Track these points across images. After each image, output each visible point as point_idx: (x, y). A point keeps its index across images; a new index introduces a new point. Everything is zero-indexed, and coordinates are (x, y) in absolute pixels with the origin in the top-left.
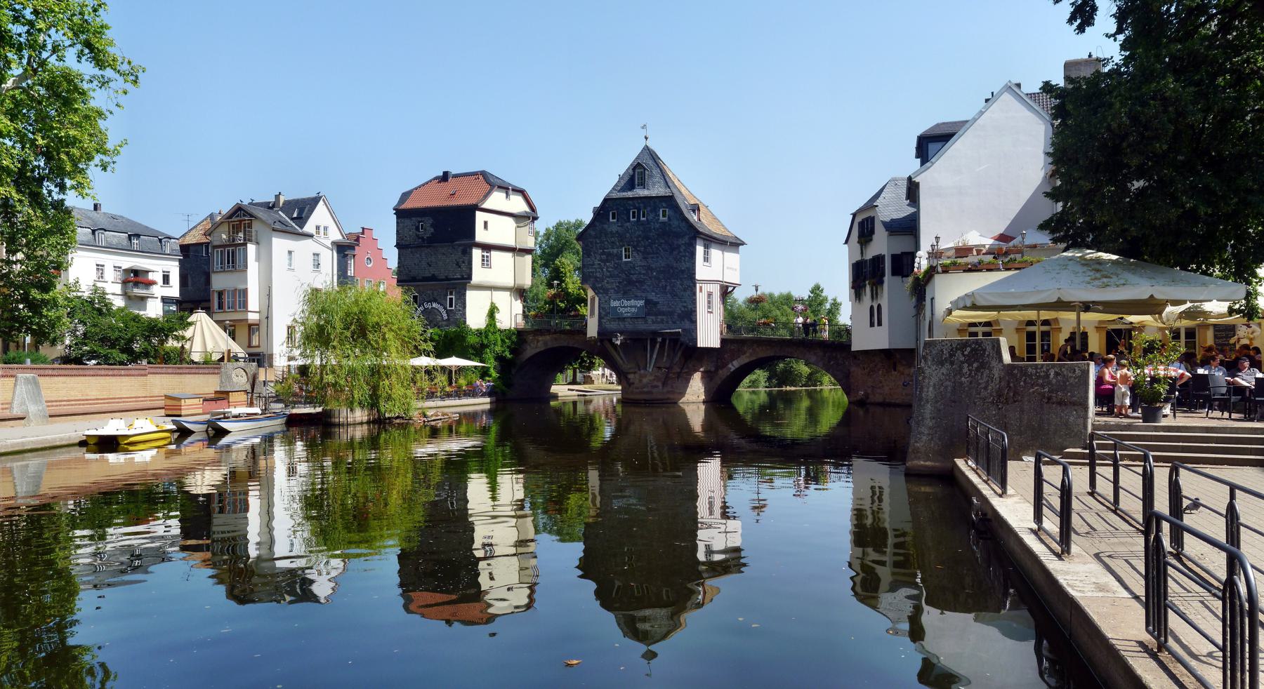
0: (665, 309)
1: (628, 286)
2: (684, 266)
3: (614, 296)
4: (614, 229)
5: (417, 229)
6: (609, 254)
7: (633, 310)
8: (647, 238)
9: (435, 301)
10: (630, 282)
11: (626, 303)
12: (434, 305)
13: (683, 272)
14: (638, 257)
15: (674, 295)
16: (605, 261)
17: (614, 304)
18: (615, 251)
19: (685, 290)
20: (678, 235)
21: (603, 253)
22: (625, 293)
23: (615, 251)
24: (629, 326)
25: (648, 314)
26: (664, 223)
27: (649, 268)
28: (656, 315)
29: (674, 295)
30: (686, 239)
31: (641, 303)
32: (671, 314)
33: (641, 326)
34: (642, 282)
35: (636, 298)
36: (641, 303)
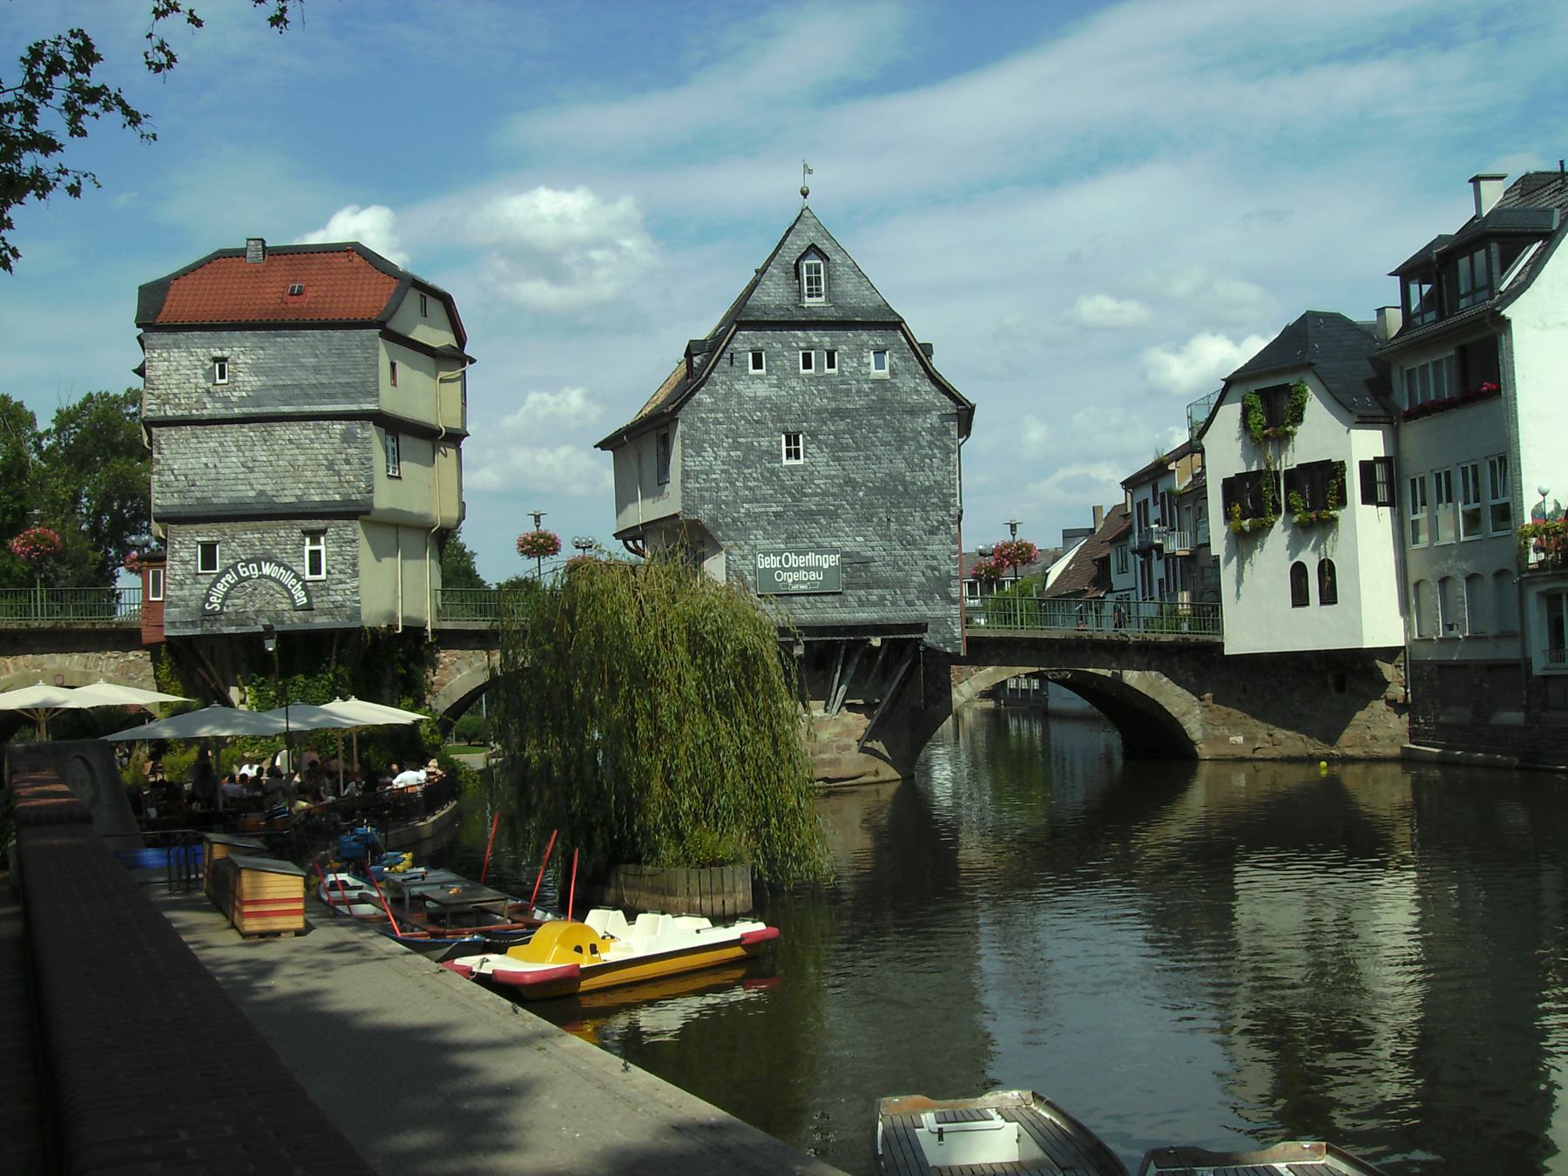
0: (887, 572)
1: (798, 520)
2: (923, 479)
3: (763, 543)
4: (761, 390)
5: (209, 375)
6: (750, 448)
7: (813, 576)
8: (839, 414)
9: (270, 560)
10: (810, 516)
11: (800, 561)
12: (267, 569)
13: (927, 491)
14: (821, 458)
15: (908, 542)
16: (741, 464)
17: (766, 562)
18: (765, 442)
19: (933, 532)
20: (913, 412)
21: (736, 446)
22: (791, 537)
23: (765, 442)
24: (805, 613)
25: (848, 586)
26: (880, 382)
27: (849, 481)
28: (868, 586)
29: (908, 542)
30: (933, 419)
31: (830, 561)
32: (904, 584)
33: (833, 613)
34: (833, 515)
35: (820, 550)
36: (830, 561)
